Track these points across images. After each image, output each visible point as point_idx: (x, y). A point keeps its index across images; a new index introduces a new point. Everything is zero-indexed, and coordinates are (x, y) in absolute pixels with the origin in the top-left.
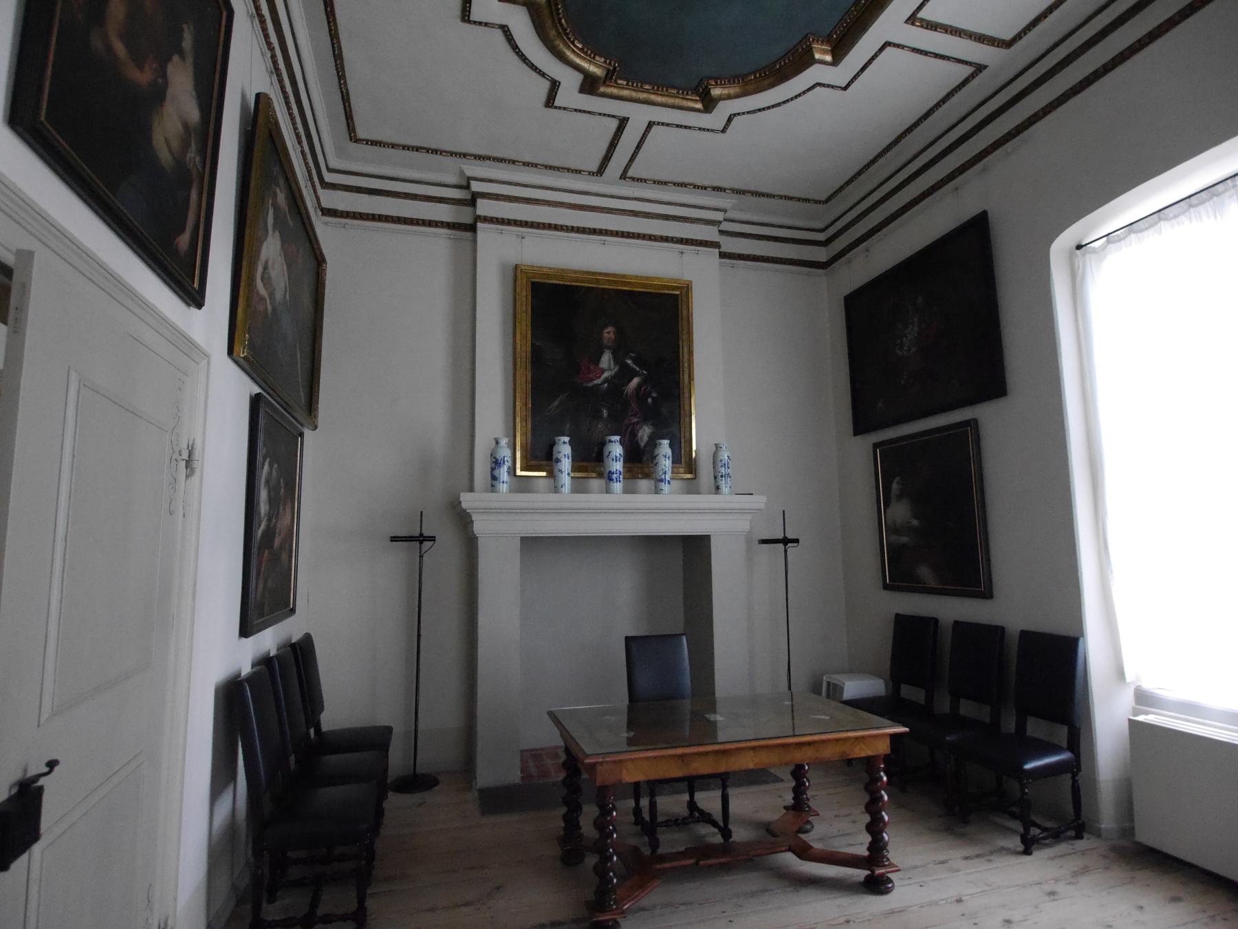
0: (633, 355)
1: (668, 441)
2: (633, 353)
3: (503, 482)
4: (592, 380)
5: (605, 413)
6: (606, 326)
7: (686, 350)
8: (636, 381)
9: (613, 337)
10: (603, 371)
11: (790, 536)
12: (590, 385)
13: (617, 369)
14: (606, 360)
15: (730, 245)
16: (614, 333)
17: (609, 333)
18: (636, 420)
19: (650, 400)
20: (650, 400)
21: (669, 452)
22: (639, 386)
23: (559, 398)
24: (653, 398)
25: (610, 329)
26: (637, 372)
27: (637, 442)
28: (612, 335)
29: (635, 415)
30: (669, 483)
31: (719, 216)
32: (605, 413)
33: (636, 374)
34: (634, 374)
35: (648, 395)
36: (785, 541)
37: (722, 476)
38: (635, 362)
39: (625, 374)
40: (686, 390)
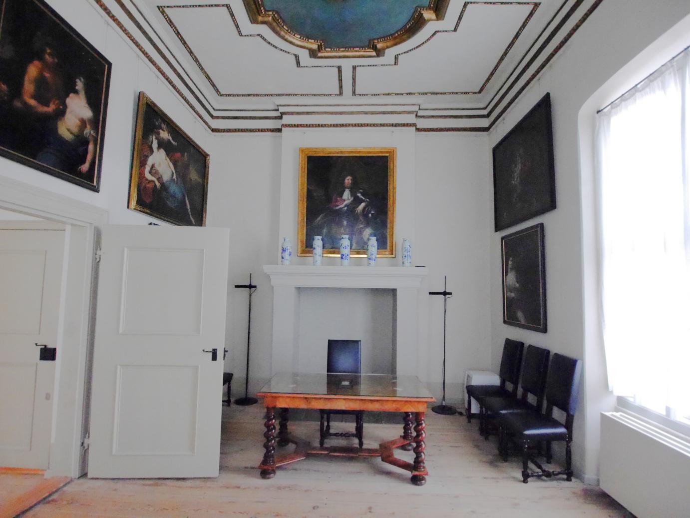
0: (361, 191)
1: (376, 238)
2: (361, 189)
3: (287, 260)
4: (338, 206)
5: (345, 223)
6: (347, 176)
7: (391, 187)
8: (363, 205)
9: (350, 182)
10: (345, 201)
11: (447, 291)
12: (337, 208)
13: (352, 198)
14: (347, 195)
15: (422, 124)
16: (351, 180)
17: (348, 180)
18: (362, 226)
19: (370, 215)
20: (370, 215)
21: (375, 243)
22: (364, 208)
23: (321, 216)
24: (372, 214)
25: (349, 178)
26: (364, 200)
27: (362, 238)
28: (350, 181)
29: (362, 224)
30: (375, 260)
31: (416, 108)
32: (345, 223)
33: (362, 201)
34: (361, 201)
35: (370, 212)
36: (445, 293)
37: (405, 257)
38: (363, 195)
39: (357, 201)
40: (391, 209)
